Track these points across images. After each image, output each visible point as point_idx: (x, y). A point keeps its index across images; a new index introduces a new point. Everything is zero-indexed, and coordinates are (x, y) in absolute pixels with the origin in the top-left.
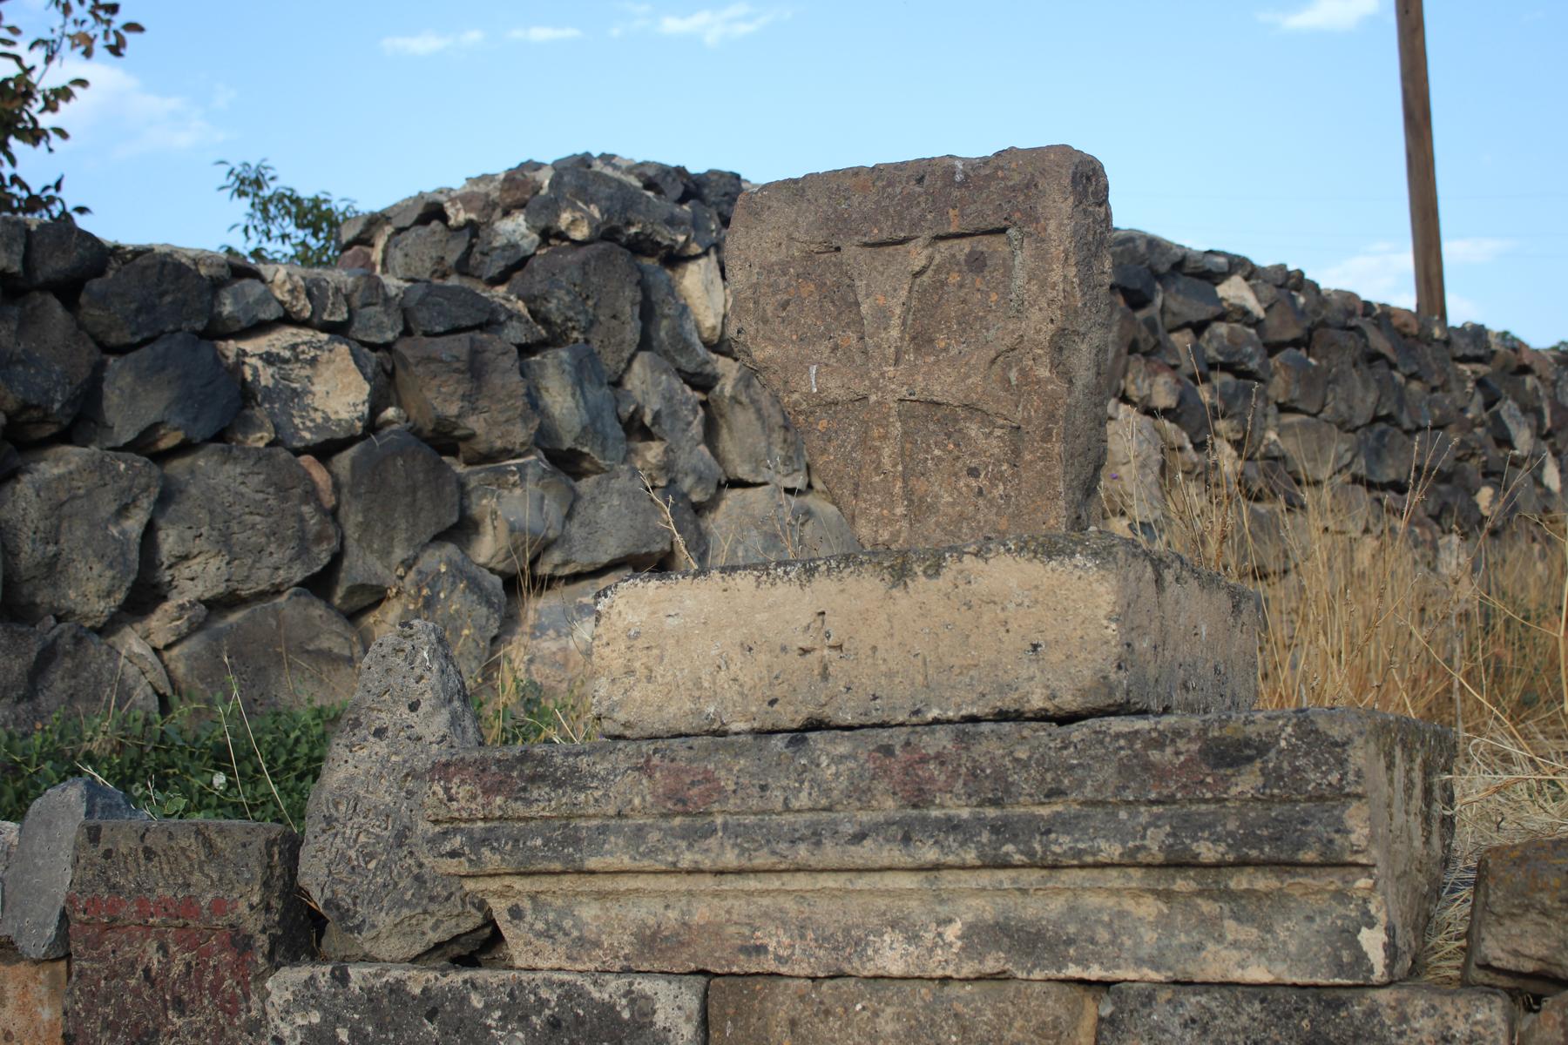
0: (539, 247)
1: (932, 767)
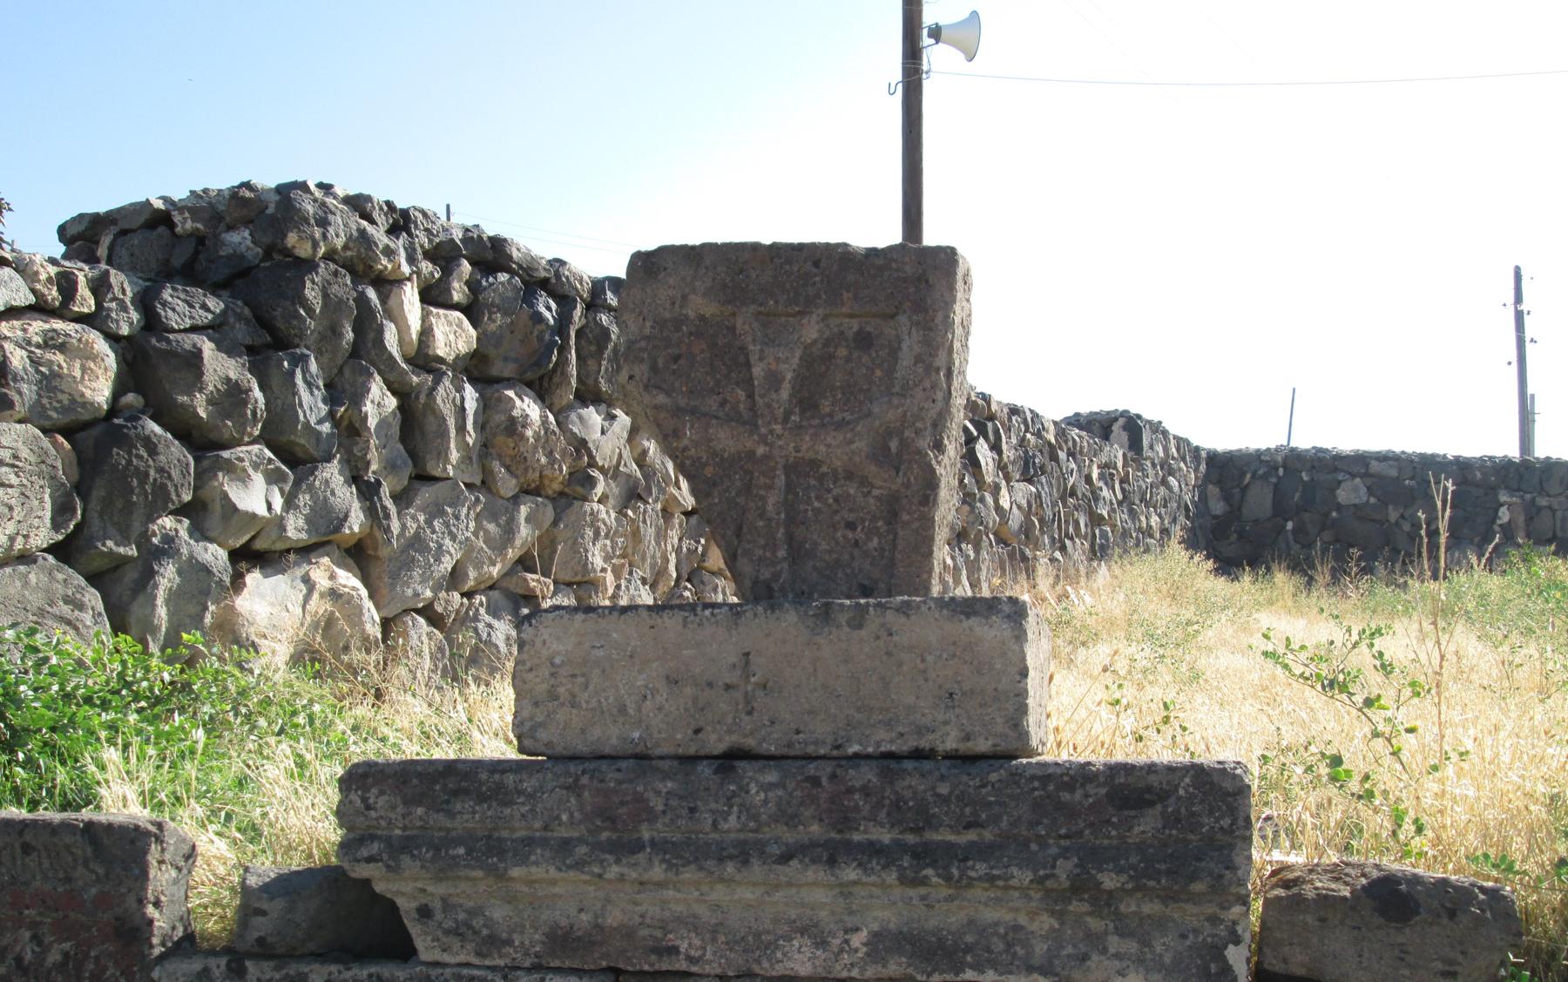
0: (262, 260)
1: (857, 796)
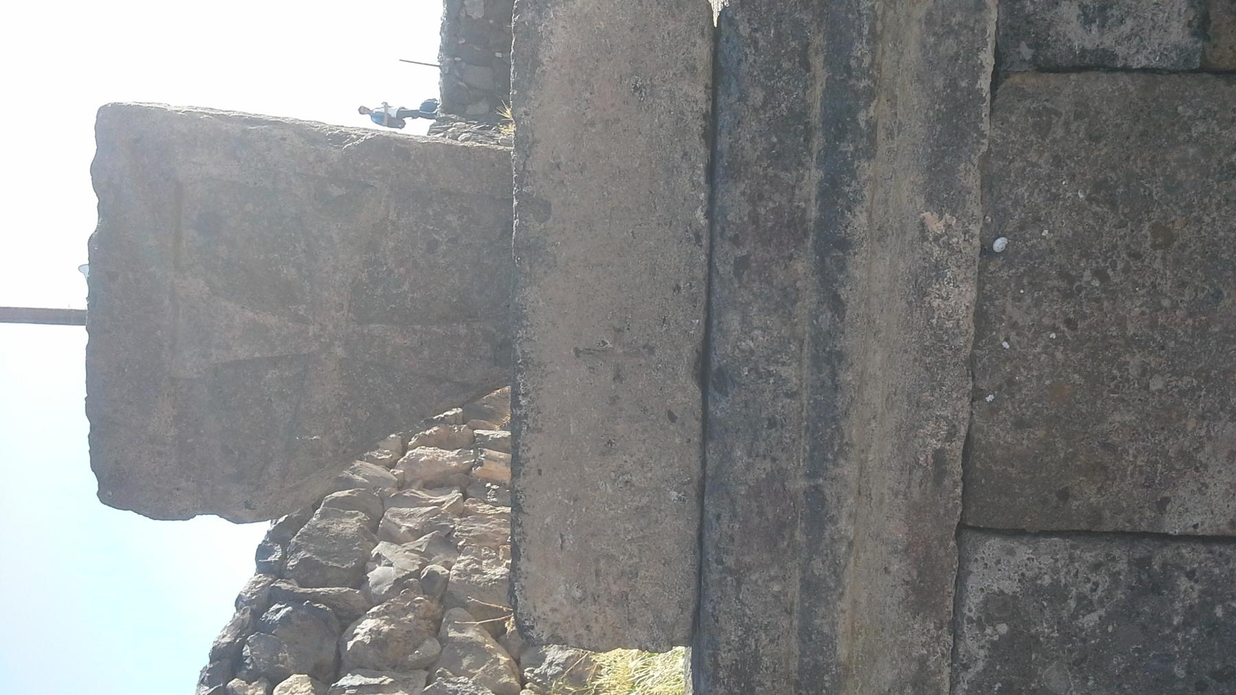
1: (763, 211)
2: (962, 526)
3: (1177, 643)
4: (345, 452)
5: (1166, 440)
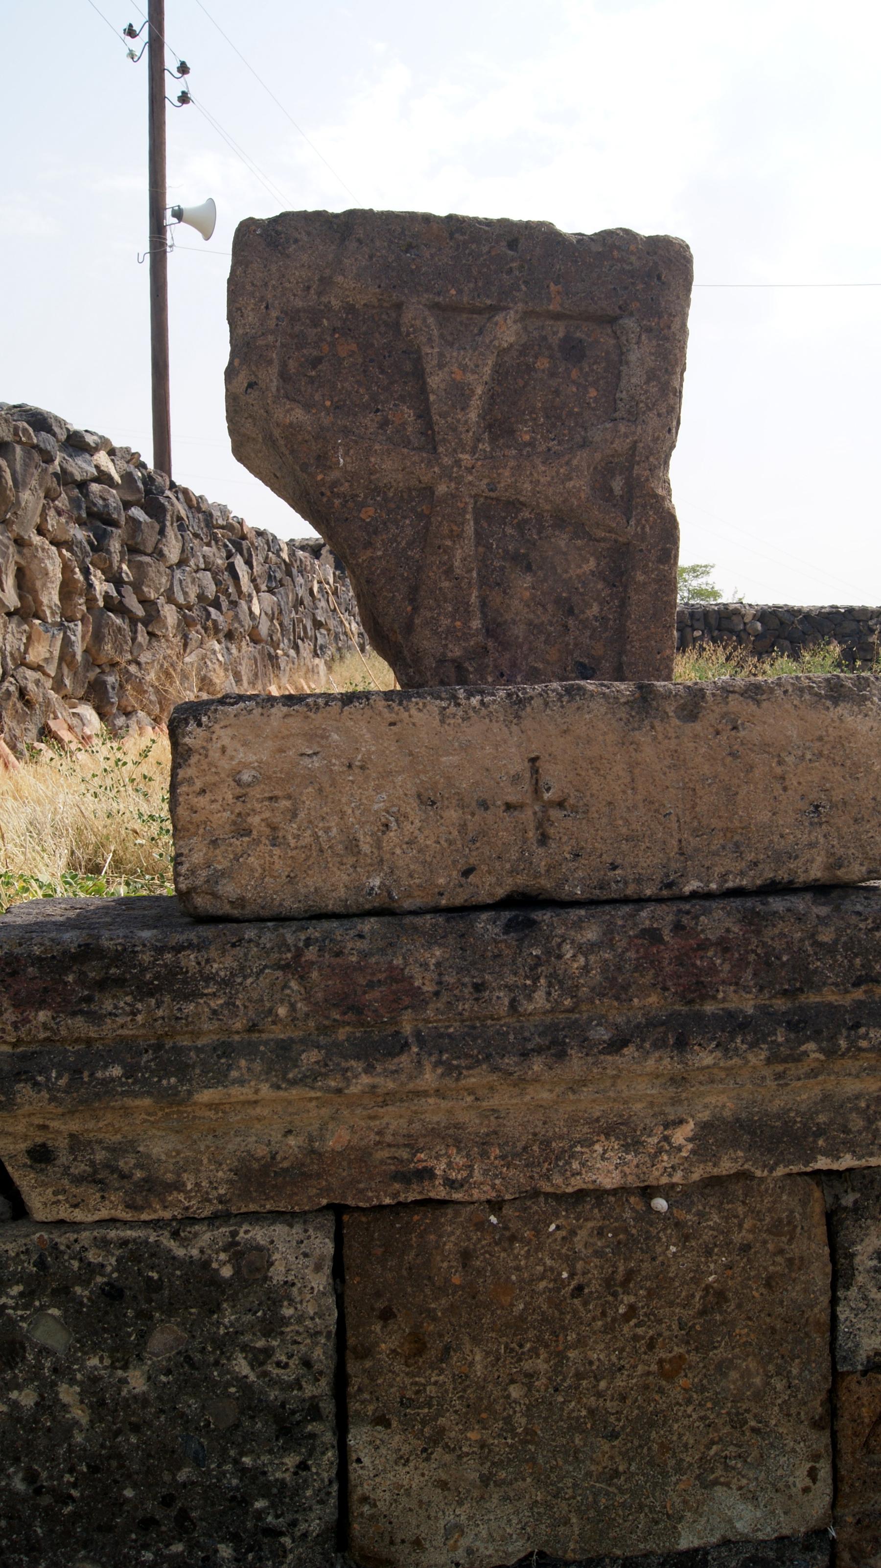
1: (710, 954)
2: (338, 1210)
3: (219, 1466)
4: (322, 494)
5: (456, 1412)
